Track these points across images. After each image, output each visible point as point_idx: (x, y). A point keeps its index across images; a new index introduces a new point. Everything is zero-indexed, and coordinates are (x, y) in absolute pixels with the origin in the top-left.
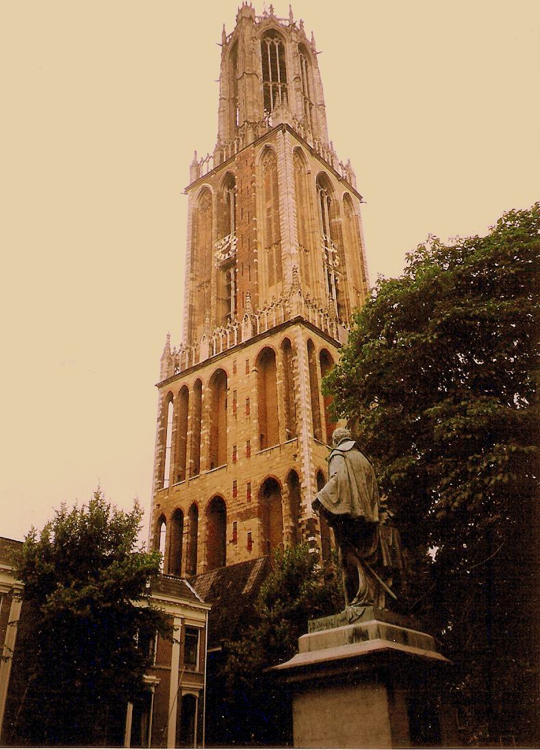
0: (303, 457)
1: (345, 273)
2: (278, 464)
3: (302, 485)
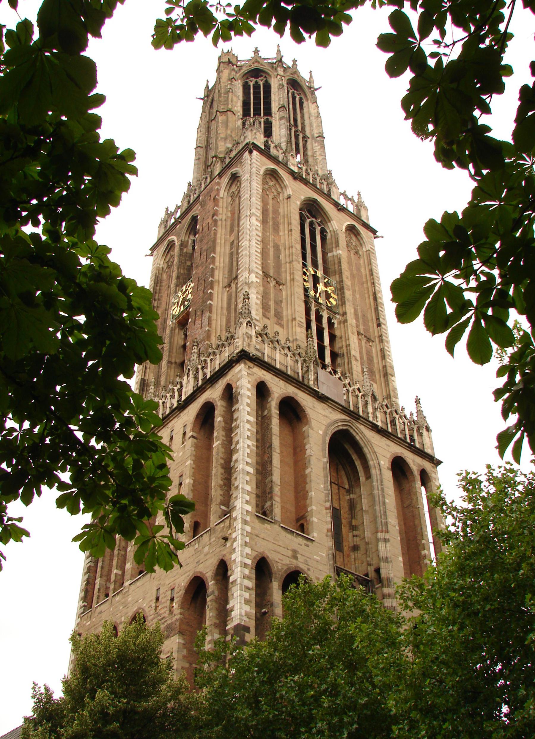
0: (235, 540)
1: (345, 314)
2: (206, 555)
3: (232, 579)
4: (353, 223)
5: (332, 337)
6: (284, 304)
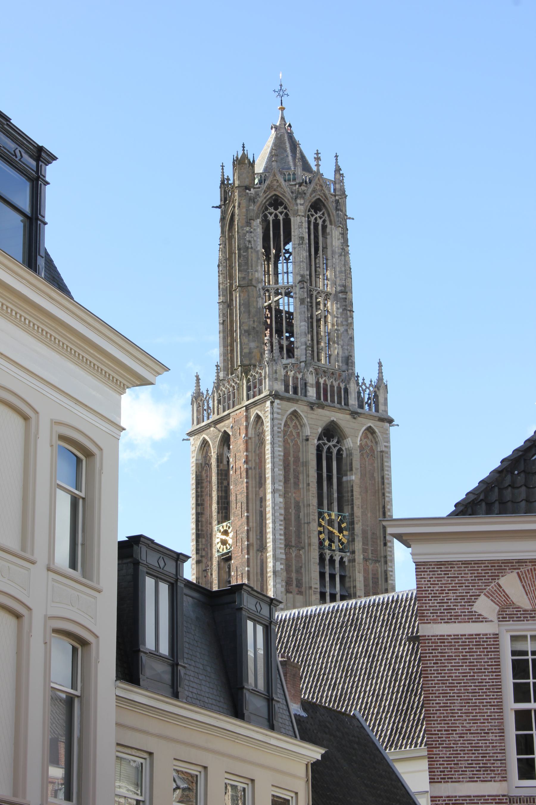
1: (353, 552)
4: (369, 425)
5: (342, 578)
6: (303, 569)
